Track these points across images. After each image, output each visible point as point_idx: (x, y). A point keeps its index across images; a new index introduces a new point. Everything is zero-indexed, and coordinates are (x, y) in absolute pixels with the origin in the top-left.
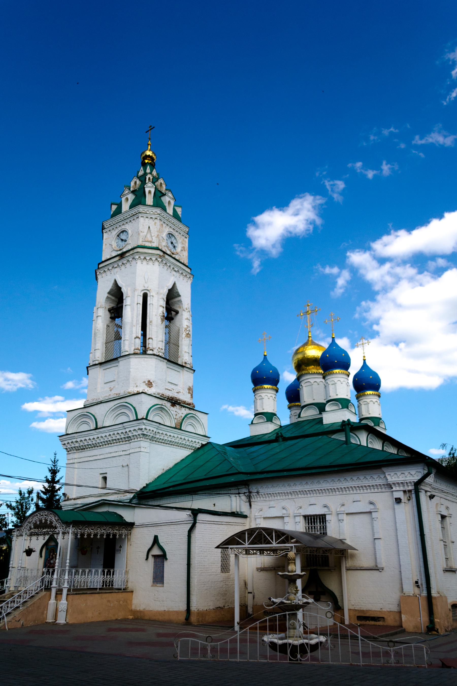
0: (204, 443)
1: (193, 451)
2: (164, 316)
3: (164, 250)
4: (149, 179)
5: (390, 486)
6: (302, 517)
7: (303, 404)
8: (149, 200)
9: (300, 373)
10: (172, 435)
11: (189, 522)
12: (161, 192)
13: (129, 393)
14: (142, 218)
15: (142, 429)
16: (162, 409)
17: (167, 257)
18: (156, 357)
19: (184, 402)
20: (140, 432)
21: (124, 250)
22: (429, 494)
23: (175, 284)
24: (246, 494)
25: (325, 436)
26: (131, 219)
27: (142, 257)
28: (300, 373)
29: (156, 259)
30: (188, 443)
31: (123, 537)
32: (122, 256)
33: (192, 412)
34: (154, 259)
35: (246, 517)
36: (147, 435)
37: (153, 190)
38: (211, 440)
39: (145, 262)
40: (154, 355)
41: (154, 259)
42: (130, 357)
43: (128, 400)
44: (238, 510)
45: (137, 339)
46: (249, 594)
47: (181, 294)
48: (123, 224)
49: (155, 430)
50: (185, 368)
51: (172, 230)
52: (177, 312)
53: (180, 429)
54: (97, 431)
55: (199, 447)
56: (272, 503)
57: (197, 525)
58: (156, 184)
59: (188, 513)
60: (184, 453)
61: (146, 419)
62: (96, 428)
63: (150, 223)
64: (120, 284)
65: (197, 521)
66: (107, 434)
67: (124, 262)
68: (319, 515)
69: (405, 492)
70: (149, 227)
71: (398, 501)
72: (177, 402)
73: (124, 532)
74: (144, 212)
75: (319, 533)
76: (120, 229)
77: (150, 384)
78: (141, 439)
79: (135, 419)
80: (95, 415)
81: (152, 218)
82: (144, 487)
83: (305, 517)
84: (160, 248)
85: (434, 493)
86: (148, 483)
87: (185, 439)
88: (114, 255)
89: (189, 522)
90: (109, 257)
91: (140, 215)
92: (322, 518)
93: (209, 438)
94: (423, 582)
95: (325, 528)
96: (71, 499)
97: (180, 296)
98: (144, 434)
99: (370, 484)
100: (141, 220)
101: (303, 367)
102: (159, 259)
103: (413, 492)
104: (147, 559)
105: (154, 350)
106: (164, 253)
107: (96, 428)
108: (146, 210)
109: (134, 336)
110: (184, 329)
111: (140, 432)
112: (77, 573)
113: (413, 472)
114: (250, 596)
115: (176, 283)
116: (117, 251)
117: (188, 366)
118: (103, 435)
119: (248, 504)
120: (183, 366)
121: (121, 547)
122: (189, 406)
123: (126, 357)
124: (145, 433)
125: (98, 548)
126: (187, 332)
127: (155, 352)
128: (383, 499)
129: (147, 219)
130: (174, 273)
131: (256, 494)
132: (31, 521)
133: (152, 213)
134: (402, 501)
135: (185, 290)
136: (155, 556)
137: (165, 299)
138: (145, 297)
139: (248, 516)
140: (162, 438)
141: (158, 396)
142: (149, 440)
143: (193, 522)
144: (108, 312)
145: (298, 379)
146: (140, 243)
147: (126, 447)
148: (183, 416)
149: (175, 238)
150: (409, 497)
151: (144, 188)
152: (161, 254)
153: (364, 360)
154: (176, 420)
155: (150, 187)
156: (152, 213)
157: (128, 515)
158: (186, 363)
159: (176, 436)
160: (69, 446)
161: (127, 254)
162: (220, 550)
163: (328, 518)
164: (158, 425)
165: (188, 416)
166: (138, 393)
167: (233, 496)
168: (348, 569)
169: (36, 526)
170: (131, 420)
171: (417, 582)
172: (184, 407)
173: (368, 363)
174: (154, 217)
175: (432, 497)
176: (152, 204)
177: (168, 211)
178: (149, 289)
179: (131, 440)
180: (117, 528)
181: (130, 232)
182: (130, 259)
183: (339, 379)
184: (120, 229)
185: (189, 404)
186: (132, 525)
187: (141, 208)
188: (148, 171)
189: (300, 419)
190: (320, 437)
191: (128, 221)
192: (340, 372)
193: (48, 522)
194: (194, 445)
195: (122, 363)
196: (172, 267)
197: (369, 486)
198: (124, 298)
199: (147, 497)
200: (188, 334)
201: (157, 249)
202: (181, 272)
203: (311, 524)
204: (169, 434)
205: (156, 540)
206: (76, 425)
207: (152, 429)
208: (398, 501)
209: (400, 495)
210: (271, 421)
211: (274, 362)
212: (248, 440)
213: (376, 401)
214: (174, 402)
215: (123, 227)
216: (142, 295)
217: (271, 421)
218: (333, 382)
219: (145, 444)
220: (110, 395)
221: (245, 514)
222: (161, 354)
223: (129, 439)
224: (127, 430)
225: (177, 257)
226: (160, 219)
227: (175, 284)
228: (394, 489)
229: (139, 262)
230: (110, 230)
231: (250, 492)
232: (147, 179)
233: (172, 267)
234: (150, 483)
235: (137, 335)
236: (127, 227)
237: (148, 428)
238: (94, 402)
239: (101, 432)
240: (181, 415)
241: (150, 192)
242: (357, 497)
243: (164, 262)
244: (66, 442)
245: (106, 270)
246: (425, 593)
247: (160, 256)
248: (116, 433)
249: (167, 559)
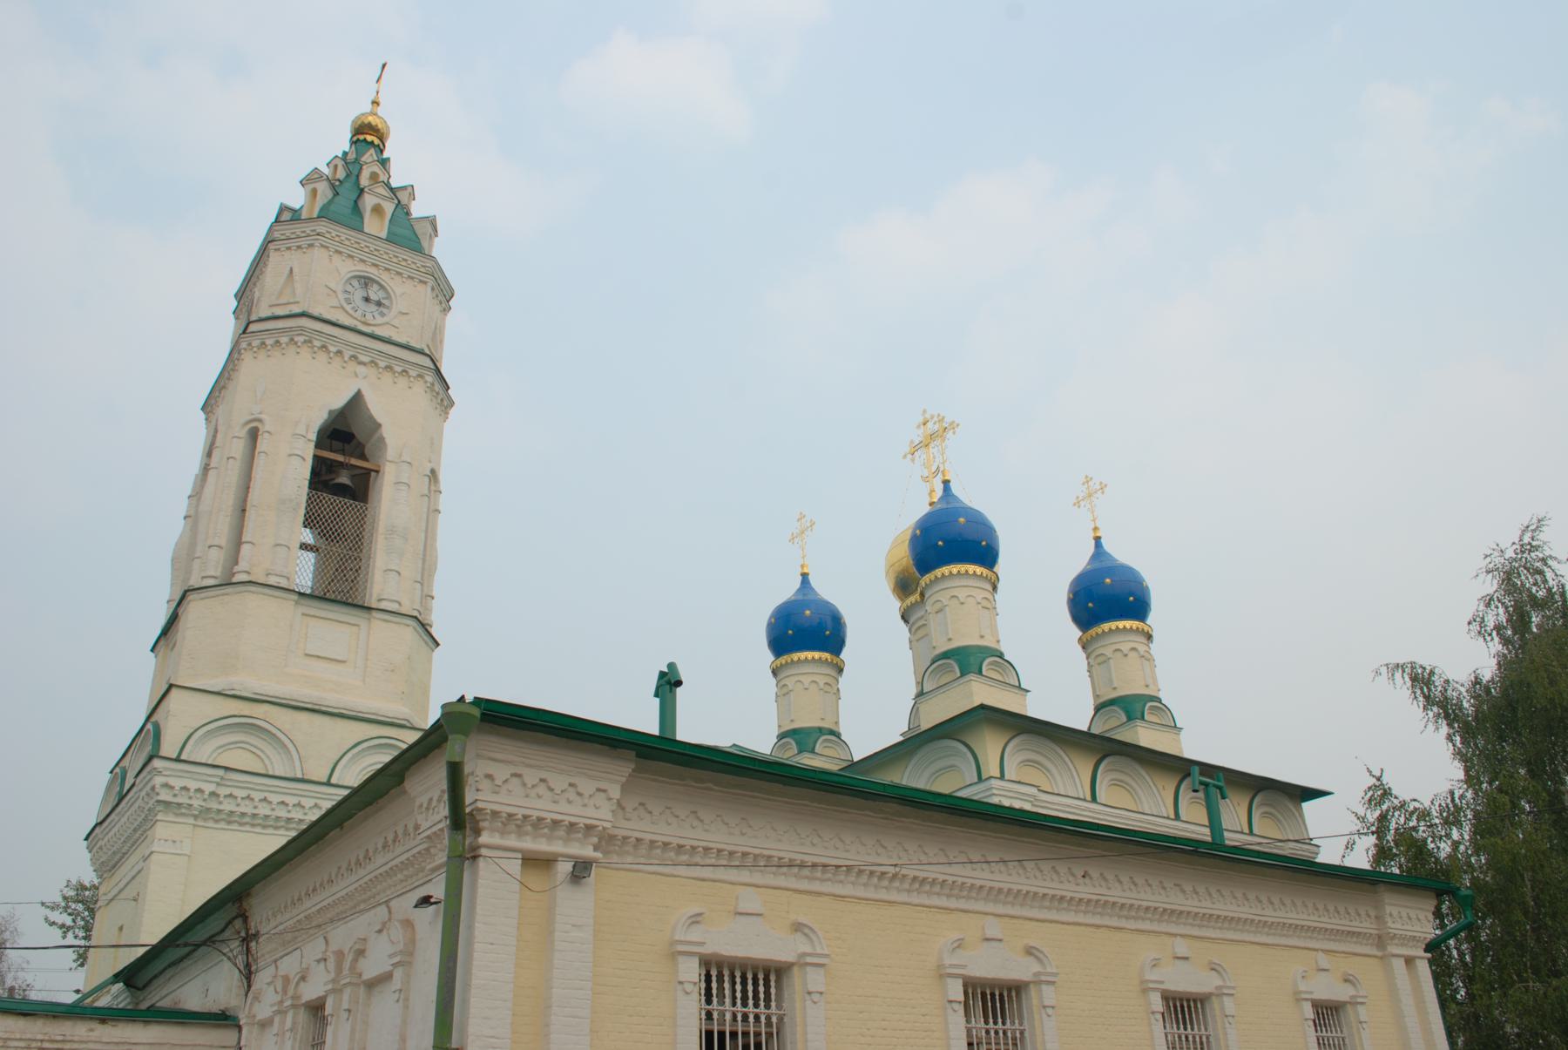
10: (291, 800)
23: (357, 398)
27: (256, 343)
36: (179, 805)
39: (262, 354)
41: (284, 340)
45: (214, 551)
47: (379, 420)
50: (374, 614)
97: (380, 425)
98: (167, 804)
115: (364, 392)
120: (369, 609)
130: (361, 370)
135: (393, 408)
140: (250, 810)
142: (191, 821)
146: (264, 312)
149: (382, 287)
153: (1097, 539)
164: (221, 772)
173: (1107, 545)
183: (955, 592)
192: (955, 571)
196: (347, 354)
204: (275, 799)
211: (827, 589)
213: (1134, 649)
216: (243, 433)
218: (938, 606)
233: (347, 354)
237: (177, 783)
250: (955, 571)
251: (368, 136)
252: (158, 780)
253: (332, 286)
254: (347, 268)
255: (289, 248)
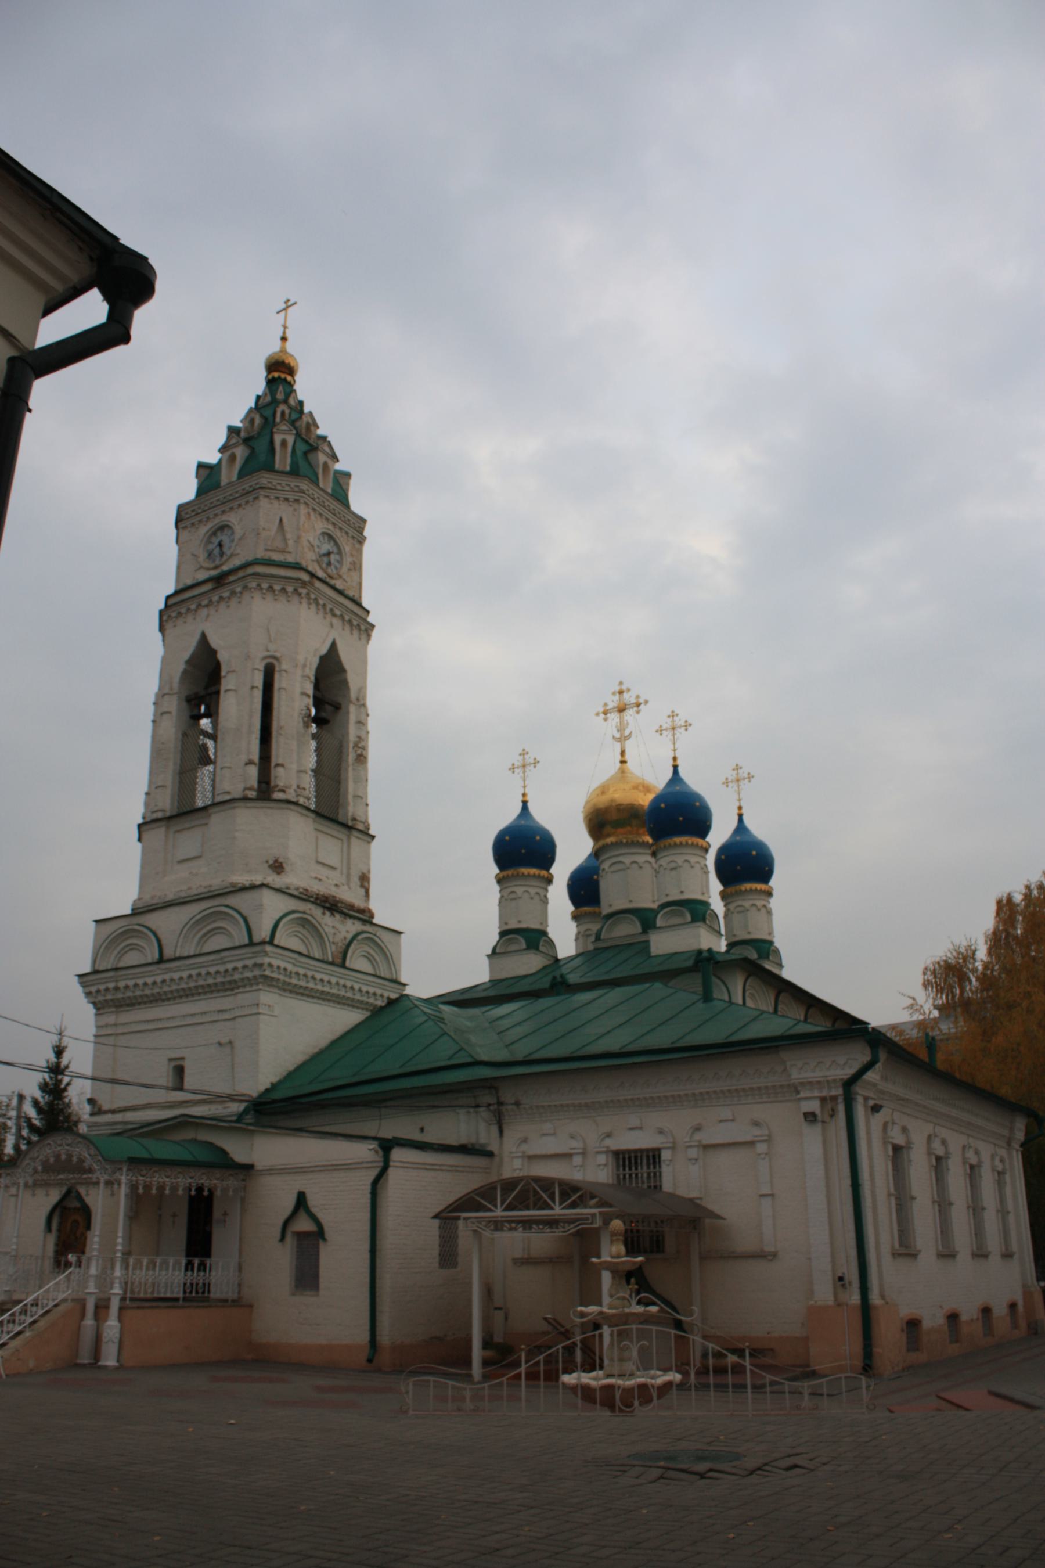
0: (394, 996)
1: (368, 1014)
2: (310, 715)
3: (310, 569)
4: (283, 413)
5: (795, 1089)
6: (610, 1155)
7: (605, 910)
8: (282, 460)
9: (601, 843)
11: (375, 1165)
12: (307, 442)
13: (233, 885)
14: (266, 500)
15: (261, 965)
16: (305, 922)
17: (318, 584)
18: (292, 807)
19: (352, 907)
20: (257, 972)
21: (225, 568)
22: (871, 1103)
23: (333, 646)
24: (492, 1108)
25: (658, 985)
26: (242, 501)
27: (265, 586)
28: (601, 843)
29: (296, 590)
30: (358, 997)
31: (231, 1193)
32: (219, 580)
33: (368, 928)
34: (290, 589)
35: (490, 1154)
36: (272, 978)
37: (290, 439)
38: (408, 991)
39: (269, 596)
40: (288, 802)
41: (290, 589)
42: (236, 805)
43: (233, 900)
44: (473, 1140)
46: (497, 1312)
48: (224, 512)
49: (290, 967)
50: (355, 833)
51: (331, 527)
52: (337, 707)
53: (343, 965)
54: (163, 966)
55: (383, 1004)
56: (547, 1127)
57: (391, 1171)
58: (298, 424)
59: (371, 1147)
60: (351, 1018)
61: (271, 942)
62: (161, 960)
63: (284, 511)
64: (214, 641)
65: (391, 1164)
66: (185, 974)
67: (226, 594)
68: (648, 1150)
69: (823, 1100)
70: (281, 520)
71: (810, 1117)
72: (336, 905)
73: (232, 1183)
74: (270, 485)
75: (645, 1186)
76: (216, 521)
77: (278, 867)
78: (260, 986)
79: (246, 941)
80: (159, 933)
81: (287, 500)
82: (267, 1090)
83: (617, 1154)
84: (304, 564)
85: (879, 1102)
86: (275, 1080)
87: (352, 988)
88: (202, 576)
89: (375, 1165)
90: (189, 582)
91: (262, 492)
92: (653, 1156)
93: (404, 985)
94: (853, 1276)
95: (658, 1176)
96: (106, 1112)
98: (266, 977)
99: (755, 1086)
100: (263, 502)
101: (608, 829)
102: (300, 590)
103: (841, 1100)
104: (282, 1239)
105: (288, 790)
106: (313, 575)
107: (161, 960)
108: (275, 482)
109: (244, 758)
110: (351, 745)
111: (257, 972)
112: (138, 1264)
113: (841, 1060)
114: (499, 1316)
116: (208, 569)
117: (361, 827)
118: (178, 973)
119: (494, 1129)
121: (225, 1214)
122: (361, 916)
123: (227, 806)
124: (267, 973)
125: (174, 1215)
126: (359, 752)
127: (291, 795)
128: (779, 1117)
129: (276, 502)
130: (335, 621)
131: (514, 1107)
132: (36, 1155)
133: (287, 488)
134: (819, 1118)
136: (300, 1236)
137: (313, 678)
138: (269, 673)
139: (496, 1152)
141: (296, 893)
142: (276, 990)
143: (382, 1164)
144: (184, 704)
145: (596, 854)
146: (260, 554)
147: (225, 1002)
148: (349, 936)
149: (336, 544)
150: (833, 1110)
151: (272, 434)
152: (305, 577)
153: (740, 816)
154: (334, 947)
155: (284, 432)
156: (287, 488)
157: (238, 1149)
158: (354, 819)
159: (334, 980)
160: (100, 998)
161: (232, 578)
162: (437, 1222)
163: (665, 1155)
165: (360, 937)
166: (253, 887)
167: (462, 1111)
168: (703, 1258)
169: (47, 1168)
170: (237, 944)
171: (841, 1279)
172: (351, 917)
173: (748, 822)
174: (291, 497)
175: (876, 1109)
176: (288, 469)
177: (321, 485)
178: (278, 655)
179: (238, 988)
180: (218, 1176)
181: (238, 530)
182: (238, 589)
183: (687, 857)
184: (216, 521)
185: (362, 911)
186: (249, 1168)
187: (265, 479)
188: (280, 396)
189: (600, 945)
190: (647, 985)
191: (235, 504)
192: (690, 842)
193: (75, 1159)
194: (371, 1000)
195: (216, 819)
196: (329, 606)
197: (752, 1089)
198: (223, 673)
199: (280, 1108)
200: (361, 755)
201: (297, 567)
202: (347, 618)
203: (630, 1169)
205: (301, 1200)
206: (116, 952)
207: (283, 965)
208: (810, 1117)
209: (814, 1106)
210: (537, 948)
211: (542, 816)
212: (485, 990)
214: (331, 905)
215: (224, 518)
216: (261, 667)
217: (537, 948)
219: (268, 997)
220: (190, 888)
221: (489, 1148)
222: (302, 801)
223: (230, 987)
224: (230, 966)
225: (339, 584)
226: (306, 503)
227: (333, 646)
228: (802, 1095)
229: (257, 595)
230: (193, 524)
231: (500, 1103)
232: (278, 415)
234: (280, 1082)
235: (251, 757)
236: (232, 518)
237: (275, 962)
238: (155, 902)
239: (170, 970)
240: (343, 934)
241: (284, 443)
242: (726, 1113)
243: (313, 596)
244: (93, 989)
245: (183, 611)
246: (855, 1298)
247: (304, 584)
248: (203, 971)
249: (324, 1240)
250: (690, 842)
251: (280, 372)
252: (267, 960)
253: (311, 539)
254: (321, 526)
255: (277, 498)
